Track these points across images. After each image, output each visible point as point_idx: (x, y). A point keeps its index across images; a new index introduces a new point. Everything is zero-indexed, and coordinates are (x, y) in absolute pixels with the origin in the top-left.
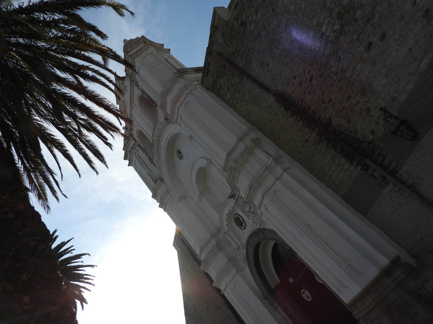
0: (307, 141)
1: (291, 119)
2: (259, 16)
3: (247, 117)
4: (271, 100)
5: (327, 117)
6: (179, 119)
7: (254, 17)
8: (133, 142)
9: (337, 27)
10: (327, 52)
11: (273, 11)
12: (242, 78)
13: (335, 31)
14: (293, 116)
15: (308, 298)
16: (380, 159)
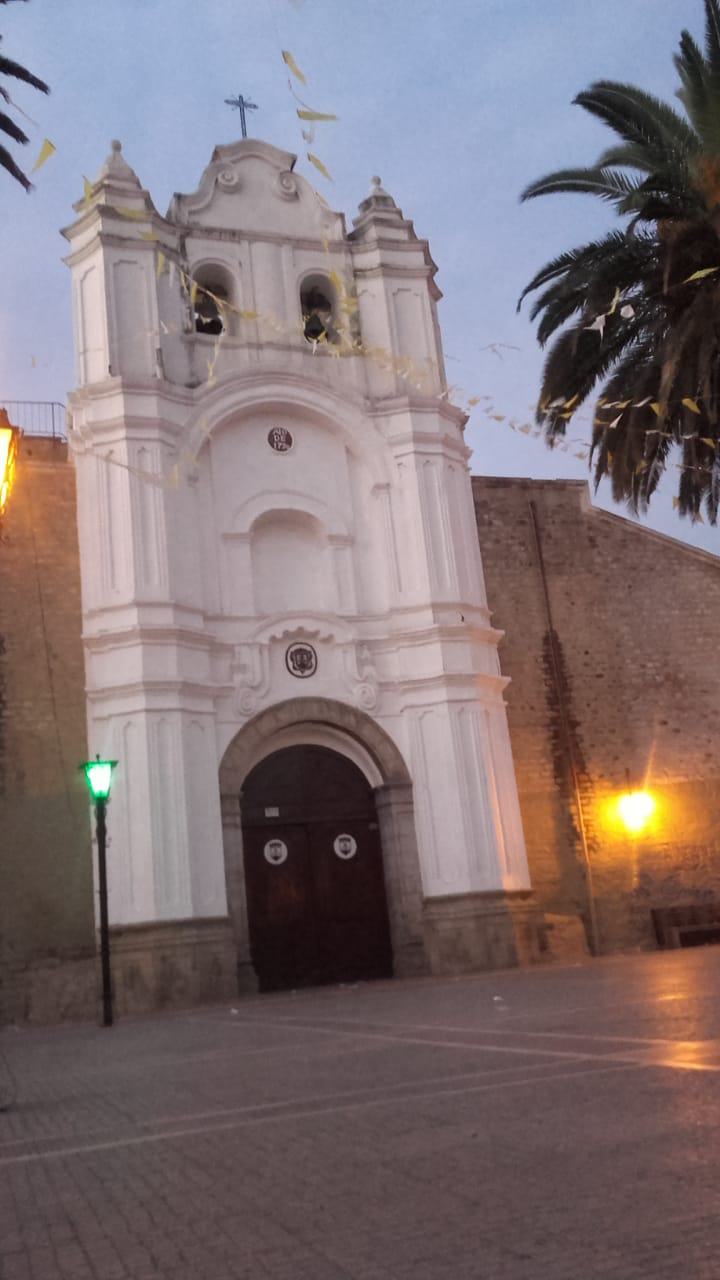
0: (532, 708)
1: (539, 672)
2: (615, 566)
3: (492, 598)
4: (539, 629)
5: (579, 719)
6: (424, 459)
7: (610, 559)
8: (173, 242)
9: (657, 678)
10: (635, 680)
11: (630, 587)
12: (530, 565)
13: (655, 679)
14: (547, 674)
15: (276, 858)
16: (585, 801)
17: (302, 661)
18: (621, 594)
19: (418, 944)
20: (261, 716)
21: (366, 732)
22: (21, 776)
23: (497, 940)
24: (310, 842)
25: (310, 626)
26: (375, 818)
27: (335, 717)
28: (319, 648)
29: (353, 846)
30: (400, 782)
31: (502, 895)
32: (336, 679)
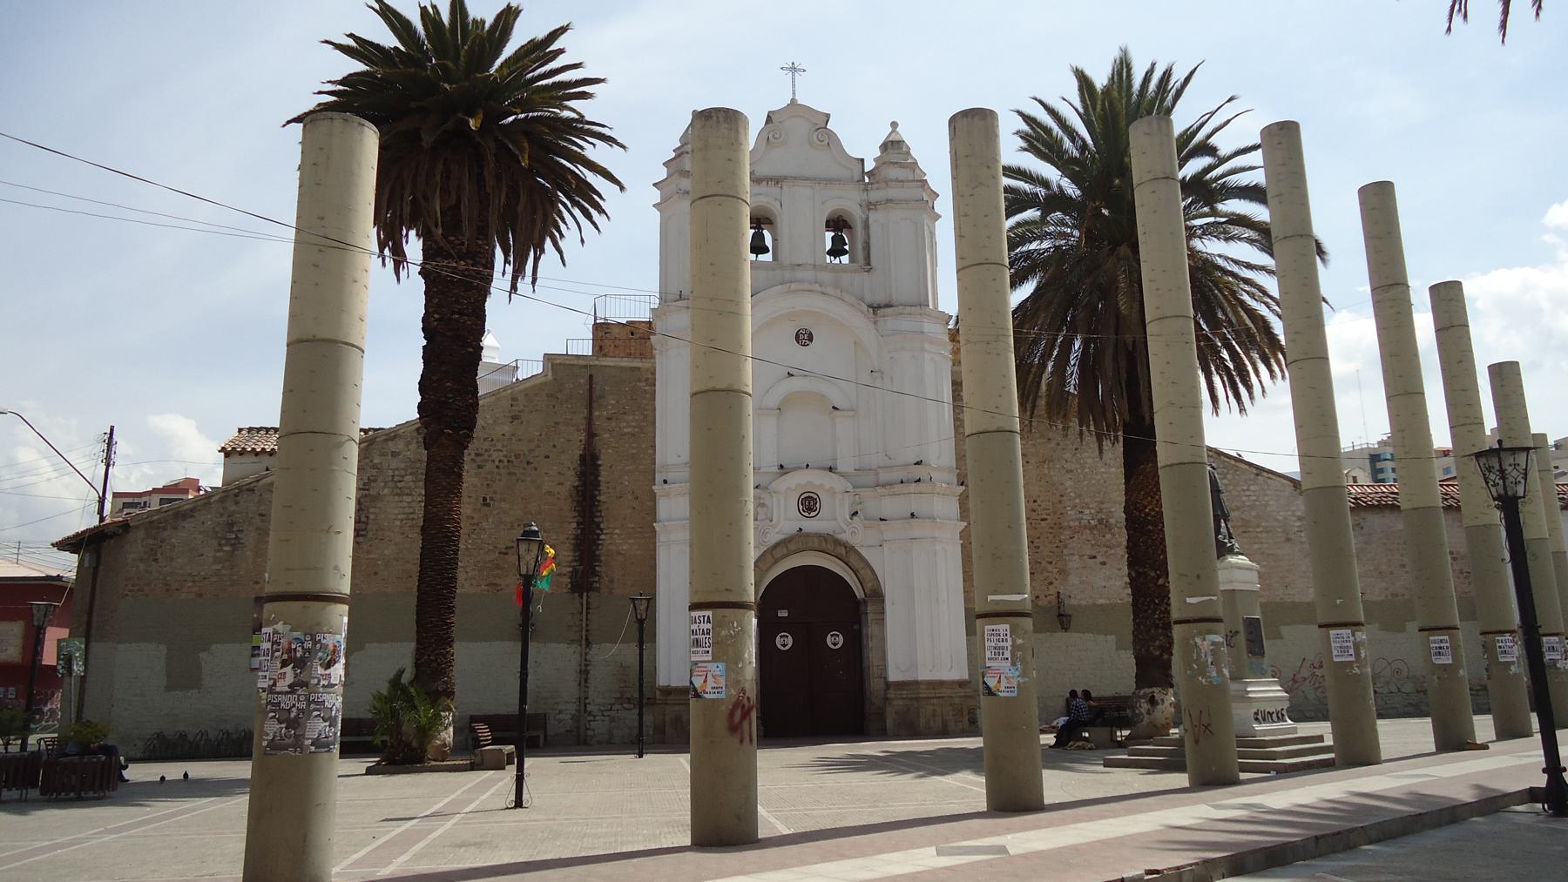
17: (809, 504)
18: (1068, 456)
19: (881, 715)
20: (777, 545)
21: (853, 559)
22: (612, 581)
23: (934, 716)
24: (810, 640)
25: (817, 482)
26: (859, 623)
27: (830, 547)
28: (825, 500)
29: (841, 640)
30: (877, 596)
31: (941, 683)
32: (831, 519)
